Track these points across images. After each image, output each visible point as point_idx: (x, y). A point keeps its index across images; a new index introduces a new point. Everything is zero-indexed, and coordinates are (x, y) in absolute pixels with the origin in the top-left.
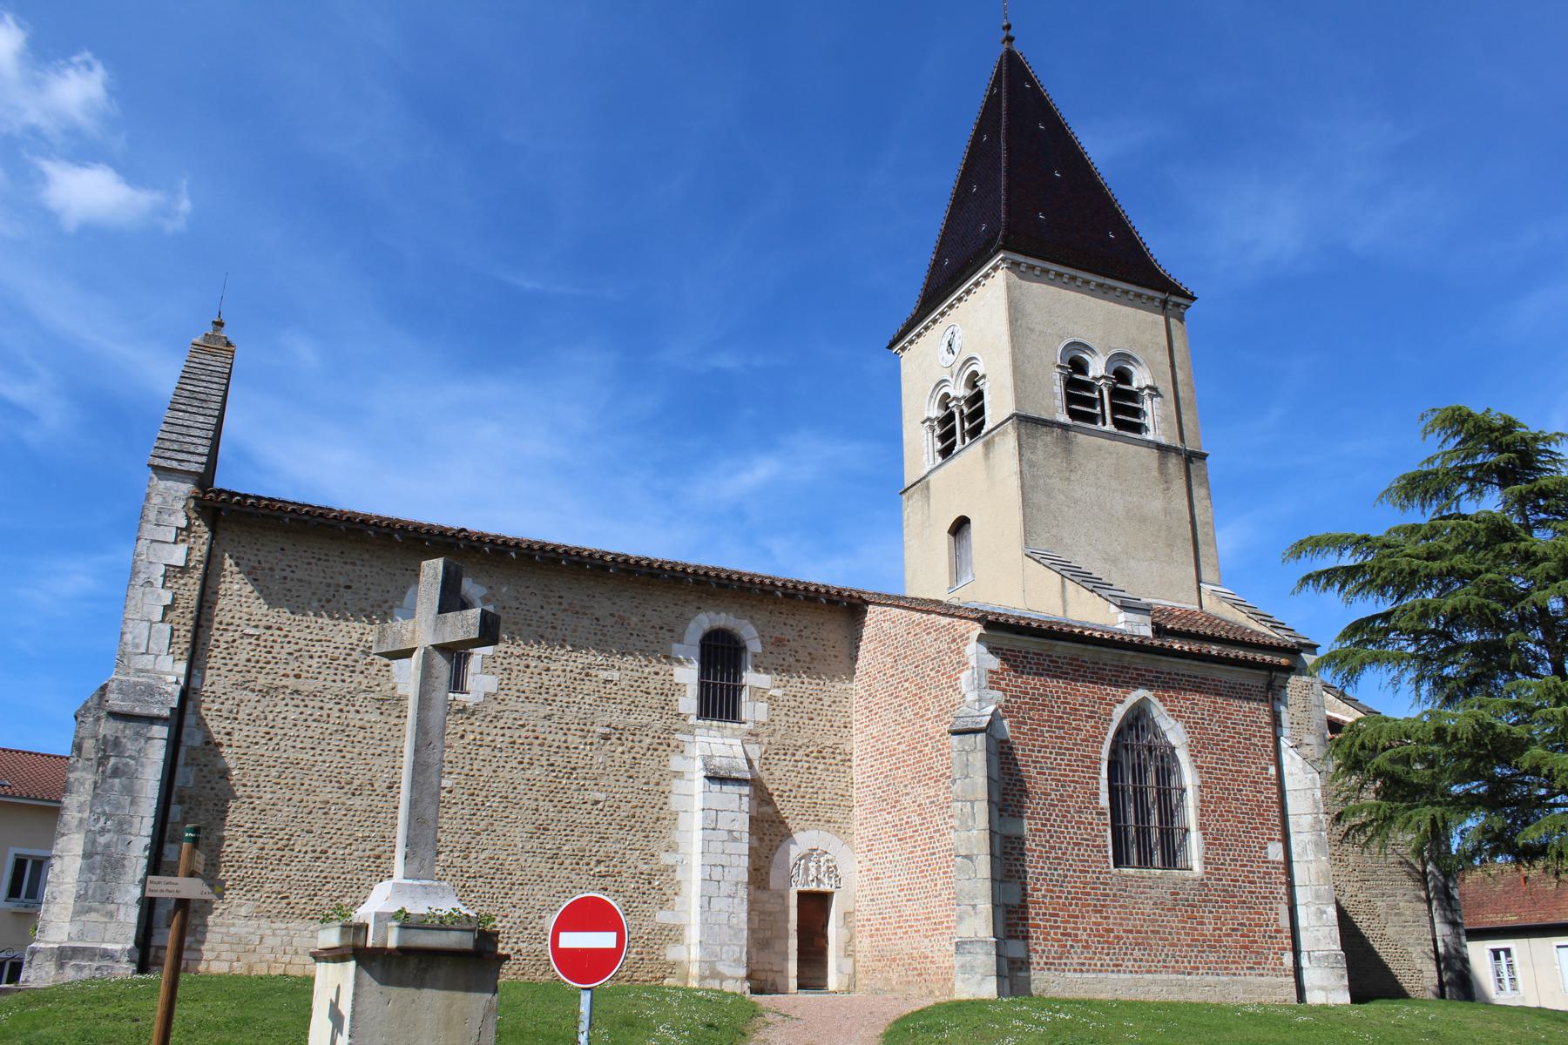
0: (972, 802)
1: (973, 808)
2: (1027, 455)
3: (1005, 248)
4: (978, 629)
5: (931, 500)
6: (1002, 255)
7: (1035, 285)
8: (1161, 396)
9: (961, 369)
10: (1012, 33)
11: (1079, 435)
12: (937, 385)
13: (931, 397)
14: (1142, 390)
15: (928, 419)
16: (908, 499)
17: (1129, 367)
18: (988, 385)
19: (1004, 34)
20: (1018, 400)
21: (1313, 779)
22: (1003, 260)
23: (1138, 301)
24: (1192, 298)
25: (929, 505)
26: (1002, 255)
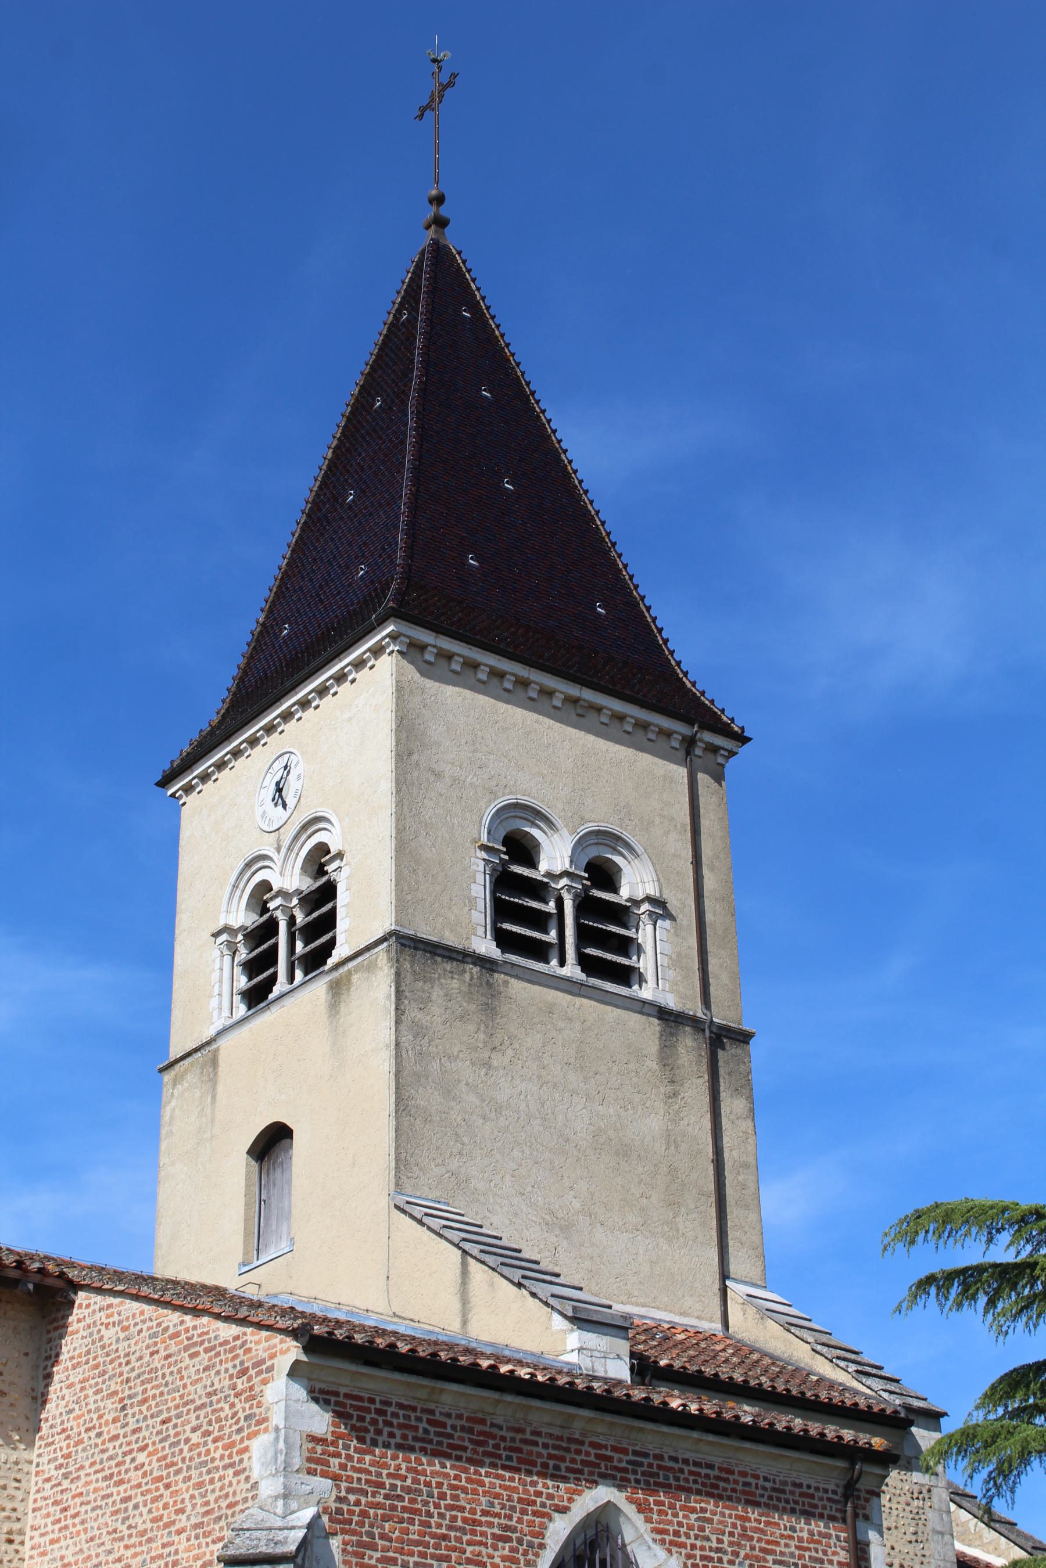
2: (412, 1013)
3: (398, 614)
4: (292, 1351)
5: (220, 1088)
6: (390, 628)
7: (450, 690)
8: (672, 918)
10: (444, 211)
11: (513, 981)
12: (248, 865)
13: (235, 886)
14: (637, 903)
15: (226, 929)
16: (175, 1082)
17: (617, 859)
18: (345, 872)
19: (430, 212)
20: (402, 905)
22: (393, 637)
23: (640, 735)
24: (742, 739)
25: (214, 1097)
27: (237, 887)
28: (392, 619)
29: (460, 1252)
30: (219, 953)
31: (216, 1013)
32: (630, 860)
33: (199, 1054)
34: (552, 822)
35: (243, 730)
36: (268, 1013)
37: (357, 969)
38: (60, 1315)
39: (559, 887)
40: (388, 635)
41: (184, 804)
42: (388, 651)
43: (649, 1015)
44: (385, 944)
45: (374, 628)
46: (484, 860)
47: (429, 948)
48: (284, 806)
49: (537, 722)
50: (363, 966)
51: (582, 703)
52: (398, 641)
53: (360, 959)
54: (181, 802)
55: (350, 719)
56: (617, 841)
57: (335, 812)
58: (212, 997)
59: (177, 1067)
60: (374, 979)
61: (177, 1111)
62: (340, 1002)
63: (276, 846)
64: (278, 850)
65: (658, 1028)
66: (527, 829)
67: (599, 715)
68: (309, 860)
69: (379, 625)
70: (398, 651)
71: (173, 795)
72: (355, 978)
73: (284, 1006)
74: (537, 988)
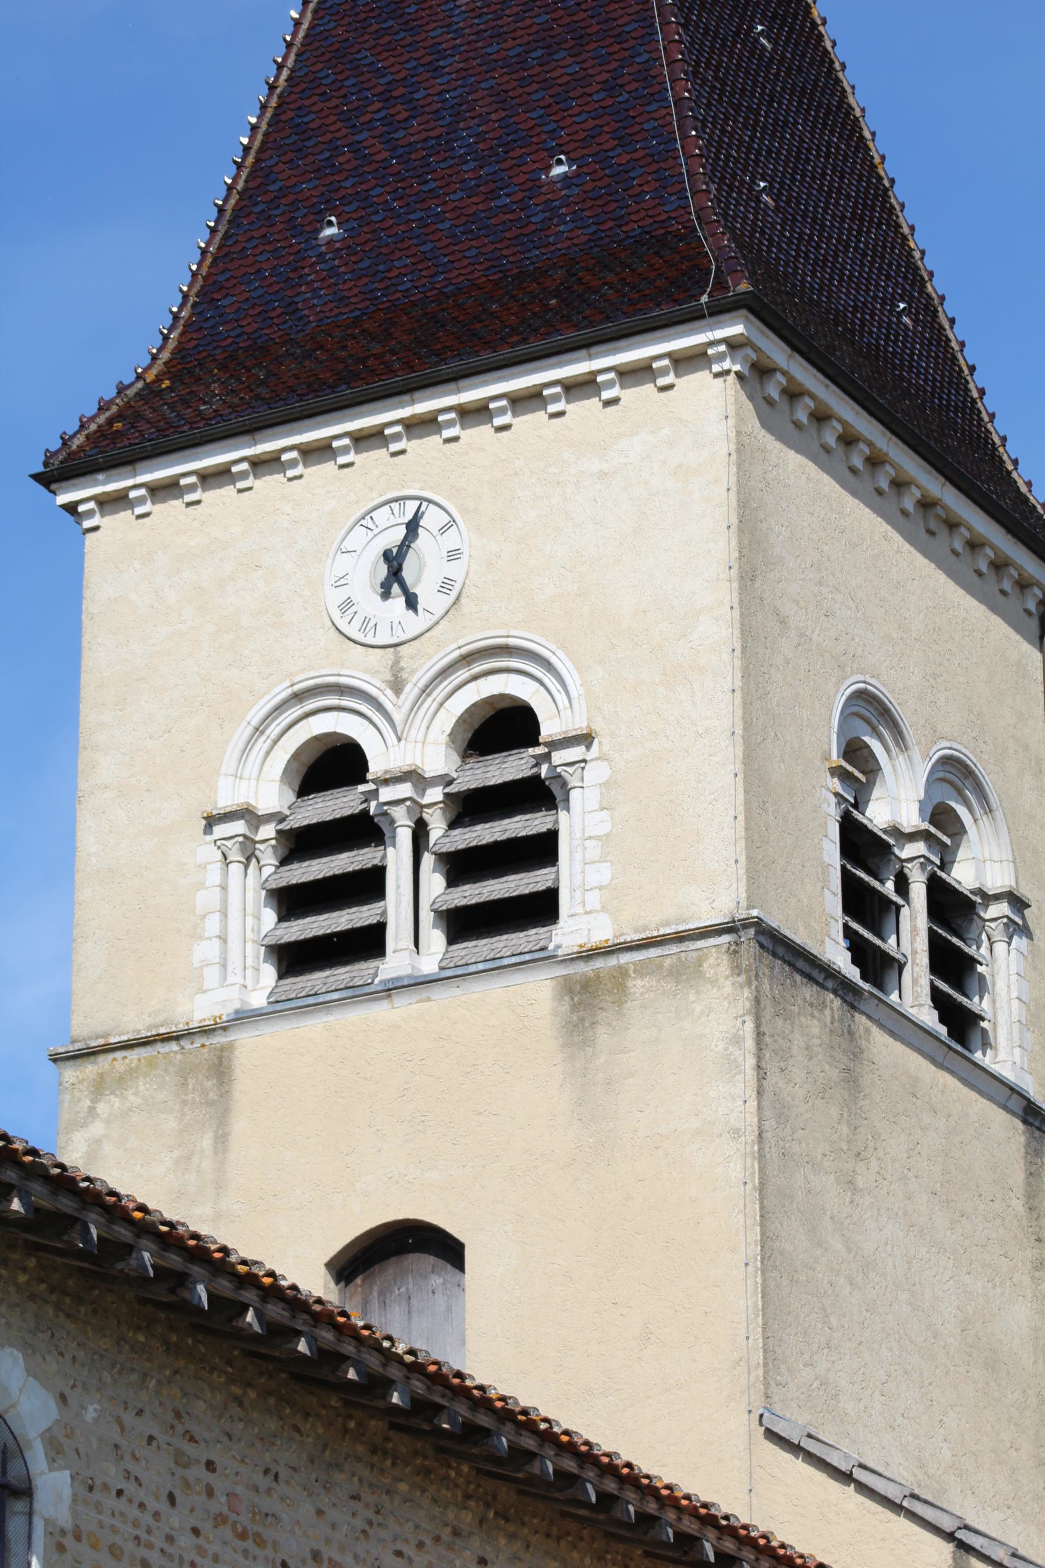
2: (774, 1079)
5: (240, 1125)
6: (735, 329)
7: (800, 459)
8: (1030, 936)
11: (875, 1029)
12: (298, 697)
13: (259, 730)
14: (989, 899)
15: (246, 813)
16: (99, 1088)
17: (961, 811)
18: (595, 773)
22: (733, 345)
23: (991, 584)
25: (222, 1140)
26: (735, 329)
27: (262, 733)
28: (744, 312)
29: (949, 1548)
30: (218, 855)
31: (212, 975)
32: (978, 816)
33: (174, 1046)
34: (900, 733)
35: (295, 425)
36: (385, 1004)
37: (642, 970)
39: (904, 855)
40: (725, 341)
41: (96, 529)
42: (716, 368)
43: (1013, 1113)
44: (726, 938)
45: (702, 317)
46: (837, 794)
47: (780, 951)
48: (412, 602)
49: (885, 537)
50: (661, 967)
51: (939, 510)
52: (740, 353)
53: (653, 952)
54: (87, 524)
55: (602, 475)
56: (966, 777)
57: (563, 647)
58: (201, 938)
59: (104, 1062)
60: (692, 997)
61: (108, 1148)
62: (594, 1023)
63: (389, 676)
64: (397, 686)
65: (1022, 1139)
66: (867, 739)
67: (951, 535)
68: (465, 721)
69: (711, 315)
70: (736, 373)
71: (71, 508)
72: (637, 985)
73: (429, 999)
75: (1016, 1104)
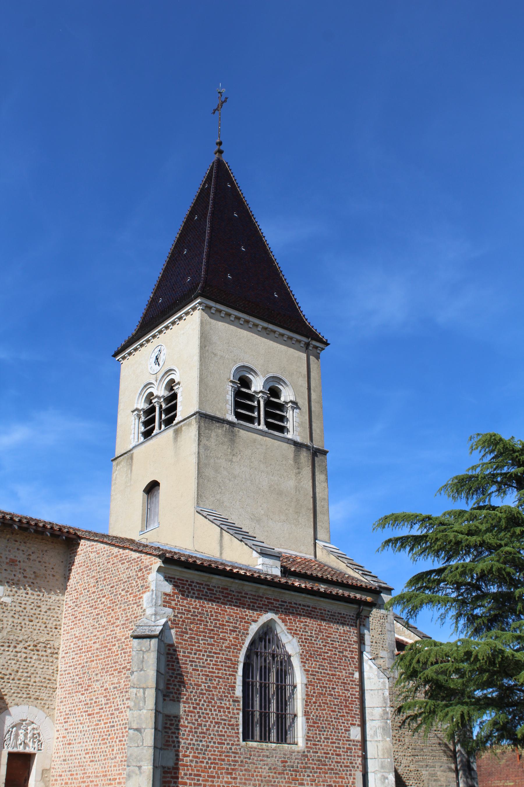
0: (144, 689)
1: (144, 693)
2: (204, 441)
3: (202, 295)
4: (158, 563)
5: (134, 468)
6: (199, 300)
7: (220, 324)
8: (300, 409)
9: (163, 376)
10: (222, 148)
11: (241, 430)
12: (145, 386)
13: (140, 394)
14: (287, 403)
15: (137, 409)
16: (117, 465)
17: (280, 387)
19: (217, 148)
21: (384, 683)
22: (200, 304)
23: (289, 342)
24: (327, 344)
25: (131, 471)
26: (199, 300)
29: (220, 528)
31: (132, 440)
37: (184, 425)
38: (74, 548)
39: (259, 396)
40: (198, 303)
43: (290, 444)
44: (195, 416)
45: (193, 300)
48: (159, 365)
49: (252, 336)
53: (185, 421)
55: (183, 333)
59: (118, 459)
61: (118, 476)
64: (156, 381)
65: (293, 449)
66: (247, 375)
71: (118, 360)
72: (183, 428)
74: (250, 433)
75: (292, 443)
